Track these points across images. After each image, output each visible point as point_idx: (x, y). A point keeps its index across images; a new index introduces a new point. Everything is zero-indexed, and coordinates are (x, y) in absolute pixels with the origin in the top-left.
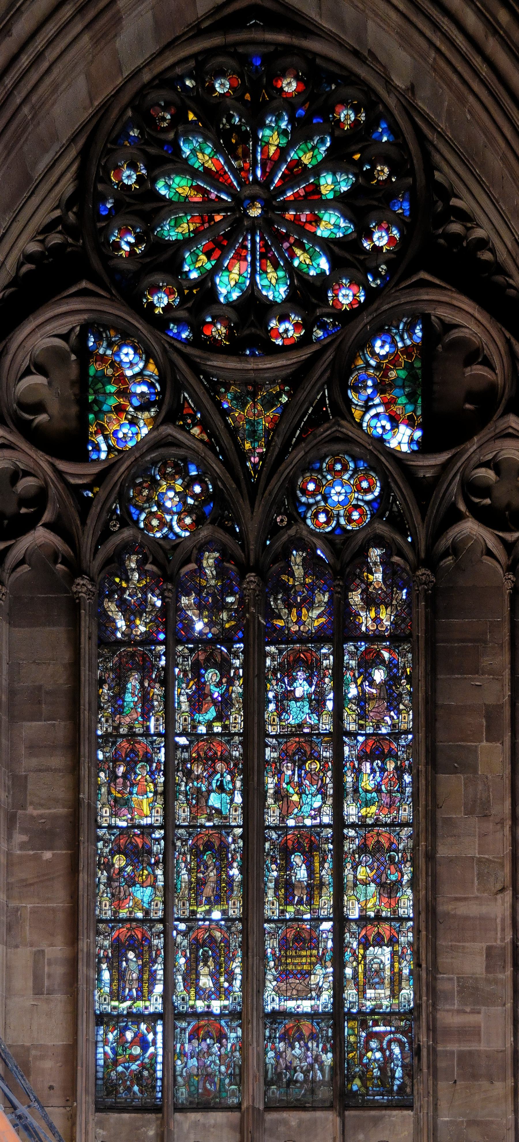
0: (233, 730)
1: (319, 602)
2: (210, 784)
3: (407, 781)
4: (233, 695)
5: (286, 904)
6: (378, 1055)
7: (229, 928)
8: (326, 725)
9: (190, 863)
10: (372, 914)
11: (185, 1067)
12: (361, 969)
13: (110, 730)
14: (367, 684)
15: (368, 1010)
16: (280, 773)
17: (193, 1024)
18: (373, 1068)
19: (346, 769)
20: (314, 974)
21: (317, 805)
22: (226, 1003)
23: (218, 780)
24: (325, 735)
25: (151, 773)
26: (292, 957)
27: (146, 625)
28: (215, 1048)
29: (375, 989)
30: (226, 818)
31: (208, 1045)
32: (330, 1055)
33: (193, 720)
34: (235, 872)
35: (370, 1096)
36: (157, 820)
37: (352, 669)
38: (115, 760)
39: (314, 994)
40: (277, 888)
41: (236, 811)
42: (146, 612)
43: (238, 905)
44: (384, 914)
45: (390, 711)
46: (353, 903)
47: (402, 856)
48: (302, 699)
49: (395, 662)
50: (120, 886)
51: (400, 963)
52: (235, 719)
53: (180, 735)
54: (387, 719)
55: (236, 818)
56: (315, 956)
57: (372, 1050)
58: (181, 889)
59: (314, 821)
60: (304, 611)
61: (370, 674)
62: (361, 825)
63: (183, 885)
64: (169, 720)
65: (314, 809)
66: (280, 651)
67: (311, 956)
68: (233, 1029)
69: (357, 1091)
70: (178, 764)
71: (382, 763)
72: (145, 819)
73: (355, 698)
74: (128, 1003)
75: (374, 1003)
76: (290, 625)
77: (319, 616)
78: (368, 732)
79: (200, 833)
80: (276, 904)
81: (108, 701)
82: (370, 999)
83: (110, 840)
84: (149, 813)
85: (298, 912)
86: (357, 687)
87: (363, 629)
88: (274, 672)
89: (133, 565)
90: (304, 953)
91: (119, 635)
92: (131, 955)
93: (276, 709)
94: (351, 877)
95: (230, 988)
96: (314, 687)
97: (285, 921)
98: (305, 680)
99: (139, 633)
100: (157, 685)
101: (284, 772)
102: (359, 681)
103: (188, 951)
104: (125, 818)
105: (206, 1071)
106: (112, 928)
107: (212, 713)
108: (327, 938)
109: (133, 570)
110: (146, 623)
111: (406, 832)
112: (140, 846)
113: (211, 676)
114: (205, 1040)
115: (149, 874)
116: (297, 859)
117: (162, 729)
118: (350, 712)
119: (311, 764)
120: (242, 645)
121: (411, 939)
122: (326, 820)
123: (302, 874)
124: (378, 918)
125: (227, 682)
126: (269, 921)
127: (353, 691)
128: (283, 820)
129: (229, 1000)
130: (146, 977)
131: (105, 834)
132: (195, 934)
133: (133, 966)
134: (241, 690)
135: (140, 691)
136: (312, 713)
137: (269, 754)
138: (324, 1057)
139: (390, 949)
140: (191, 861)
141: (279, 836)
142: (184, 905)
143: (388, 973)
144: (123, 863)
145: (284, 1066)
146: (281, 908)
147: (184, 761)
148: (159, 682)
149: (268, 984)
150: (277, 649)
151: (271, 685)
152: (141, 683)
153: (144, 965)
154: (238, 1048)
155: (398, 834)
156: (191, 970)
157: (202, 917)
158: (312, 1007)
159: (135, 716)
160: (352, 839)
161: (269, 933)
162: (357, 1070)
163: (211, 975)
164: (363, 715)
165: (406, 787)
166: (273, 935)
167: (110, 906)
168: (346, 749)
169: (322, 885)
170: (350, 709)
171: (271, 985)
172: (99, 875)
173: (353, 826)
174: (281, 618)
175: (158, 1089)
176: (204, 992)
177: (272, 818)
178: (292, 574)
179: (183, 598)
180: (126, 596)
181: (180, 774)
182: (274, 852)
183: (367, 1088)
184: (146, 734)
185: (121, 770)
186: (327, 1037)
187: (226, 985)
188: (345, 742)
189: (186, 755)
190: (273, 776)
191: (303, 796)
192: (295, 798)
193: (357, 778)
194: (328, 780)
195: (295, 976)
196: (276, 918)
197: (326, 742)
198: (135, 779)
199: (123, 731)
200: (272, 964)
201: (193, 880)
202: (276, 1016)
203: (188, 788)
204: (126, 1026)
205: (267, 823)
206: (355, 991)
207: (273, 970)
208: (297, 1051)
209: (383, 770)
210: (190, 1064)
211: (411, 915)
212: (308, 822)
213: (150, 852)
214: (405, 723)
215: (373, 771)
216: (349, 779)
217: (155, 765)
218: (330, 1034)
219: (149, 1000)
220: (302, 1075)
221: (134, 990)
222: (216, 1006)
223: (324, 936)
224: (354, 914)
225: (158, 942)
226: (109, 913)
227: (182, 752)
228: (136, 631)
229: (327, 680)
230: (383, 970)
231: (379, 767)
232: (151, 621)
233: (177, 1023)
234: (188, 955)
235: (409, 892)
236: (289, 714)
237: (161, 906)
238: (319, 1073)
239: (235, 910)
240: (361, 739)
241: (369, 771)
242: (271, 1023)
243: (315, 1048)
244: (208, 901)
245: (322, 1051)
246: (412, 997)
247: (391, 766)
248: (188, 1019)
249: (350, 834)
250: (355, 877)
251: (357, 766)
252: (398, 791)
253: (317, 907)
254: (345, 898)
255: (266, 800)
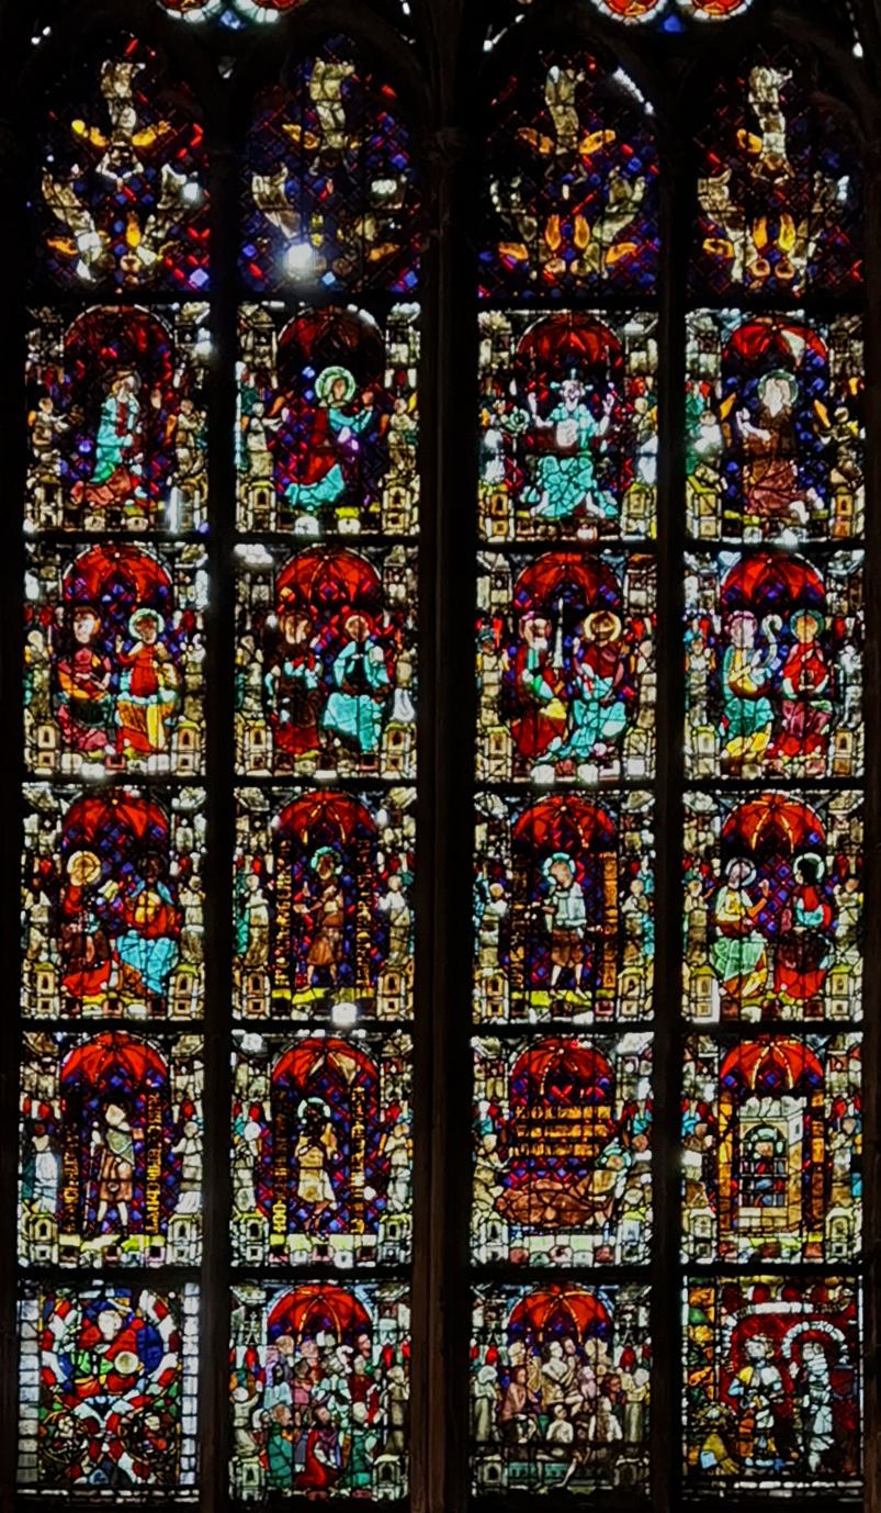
0: (391, 530)
1: (619, 201)
2: (328, 669)
3: (850, 670)
4: (392, 438)
5: (532, 986)
6: (770, 1375)
7: (377, 1048)
8: (640, 523)
9: (274, 877)
10: (755, 1014)
11: (259, 1405)
12: (724, 1155)
13: (57, 520)
14: (746, 414)
15: (743, 1261)
16: (513, 643)
17: (282, 1294)
18: (756, 1410)
19: (689, 636)
20: (603, 1167)
21: (612, 729)
22: (370, 1240)
23: (348, 660)
24: (635, 547)
25: (171, 637)
26: (543, 1123)
27: (156, 245)
28: (339, 1360)
29: (762, 1205)
30: (370, 759)
31: (321, 1349)
32: (643, 1375)
33: (282, 499)
34: (393, 902)
35: (748, 1479)
36: (185, 762)
37: (707, 378)
38: (76, 605)
39: (600, 1218)
40: (504, 948)
41: (397, 740)
42: (157, 213)
43: (402, 987)
44: (786, 1014)
45: (807, 488)
46: (705, 987)
47: (835, 863)
48: (573, 451)
49: (820, 360)
50: (84, 935)
51: (828, 1140)
52: (397, 499)
53: (250, 538)
54: (798, 507)
55: (401, 763)
56: (605, 1122)
57: (754, 1362)
58: (249, 944)
59: (605, 772)
60: (580, 223)
61: (755, 392)
62: (729, 782)
63: (255, 932)
64: (222, 503)
65: (606, 741)
66: (518, 322)
67: (595, 1120)
68: (384, 1308)
69: (713, 1468)
70: (243, 614)
71: (786, 621)
72: (153, 759)
73: (714, 453)
74: (108, 1240)
75: (758, 1241)
76: (543, 258)
77: (622, 237)
78: (748, 540)
79: (302, 798)
80: (504, 986)
81: (53, 445)
82: (748, 1232)
83: (58, 811)
84: (162, 744)
85: (559, 1007)
86: (719, 422)
87: (737, 273)
88: (502, 379)
89: (122, 89)
90: (575, 1114)
91: (83, 271)
92: (115, 1115)
93: (508, 476)
94: (701, 917)
95: (380, 1203)
96: (606, 421)
97: (528, 1030)
98: (582, 401)
99: (136, 267)
100: (186, 406)
101: (525, 642)
102: (725, 409)
103: (267, 1106)
104: (98, 754)
105: (315, 1417)
106: (64, 1046)
107: (333, 483)
108: (637, 1075)
109: (122, 102)
110: (155, 239)
111: (850, 799)
112: (140, 830)
113: (332, 384)
114: (313, 1338)
115: (164, 902)
116: (558, 869)
117: (200, 522)
118: (700, 490)
119: (597, 621)
120: (416, 307)
121: (857, 1078)
122: (636, 768)
123: (571, 908)
124: (772, 1026)
125: (373, 402)
126: (486, 1030)
127: (708, 437)
128: (522, 767)
129: (375, 1232)
130: (154, 1172)
131: (43, 795)
132: (288, 1062)
133: (120, 1144)
134: (412, 425)
135: (138, 418)
136: (601, 488)
137: (487, 595)
138: (626, 1380)
139: (803, 1101)
140: (276, 872)
141: (512, 808)
142: (256, 985)
143: (795, 1165)
144: (94, 875)
145: (520, 1405)
146: (516, 995)
147: (260, 610)
148: (189, 398)
149: (479, 1191)
150: (509, 318)
151: (494, 411)
152: (143, 397)
153: (150, 1141)
154: (399, 1356)
155: (826, 807)
156: (275, 1156)
157: (304, 1017)
158: (596, 1250)
159: (125, 484)
160: (704, 819)
161: (483, 1061)
162: (714, 1413)
163: (328, 1166)
164: (734, 499)
165: (846, 685)
166: (493, 1067)
167: (58, 985)
168: (691, 584)
169: (623, 938)
170: (700, 480)
171: (485, 1197)
172: (29, 903)
173: (707, 785)
174: (520, 240)
175: (185, 1463)
176: (311, 1213)
177: (493, 762)
178: (547, 128)
179: (257, 178)
180: (102, 169)
181: (247, 642)
182: (498, 851)
183: (740, 1461)
184: (156, 535)
185: (87, 627)
186: (636, 1329)
187: (370, 1193)
188: (688, 567)
189: (263, 592)
190: (498, 654)
191: (577, 703)
192: (555, 710)
193: (719, 658)
194: (642, 665)
195: (551, 1172)
196: (501, 1022)
197: (639, 566)
198: (125, 653)
199: (94, 523)
200: (490, 1141)
201: (281, 920)
202: (505, 1273)
203: (269, 677)
204: (102, 1298)
205: (480, 775)
206: (709, 1212)
207: (494, 1157)
208: (556, 1367)
209: (786, 639)
210: (270, 1402)
211: (859, 1017)
212: (589, 774)
213: (167, 842)
214: (845, 518)
215: (761, 642)
216: (698, 663)
217: (178, 615)
218: (643, 1323)
219: (164, 1233)
220: (568, 1427)
221: (122, 1207)
222: (342, 1249)
223: (629, 1068)
224: (706, 1009)
225: (191, 1083)
226: (55, 1003)
227: (253, 583)
228: (131, 262)
229: (640, 404)
230: (784, 1154)
231: (774, 631)
232: (169, 237)
233: (237, 1292)
234: (268, 1117)
235: (853, 956)
236: (540, 491)
237: (197, 989)
238: (613, 1423)
239: (394, 1005)
240: (730, 559)
241: (749, 642)
242: (488, 1293)
243: (603, 1358)
244: (323, 979)
245: (623, 1364)
246: (858, 1227)
247: (806, 630)
248: (267, 1283)
249: (699, 806)
250: (711, 914)
251: (718, 629)
252: (824, 695)
253: (611, 994)
254: (686, 971)
255: (477, 715)
